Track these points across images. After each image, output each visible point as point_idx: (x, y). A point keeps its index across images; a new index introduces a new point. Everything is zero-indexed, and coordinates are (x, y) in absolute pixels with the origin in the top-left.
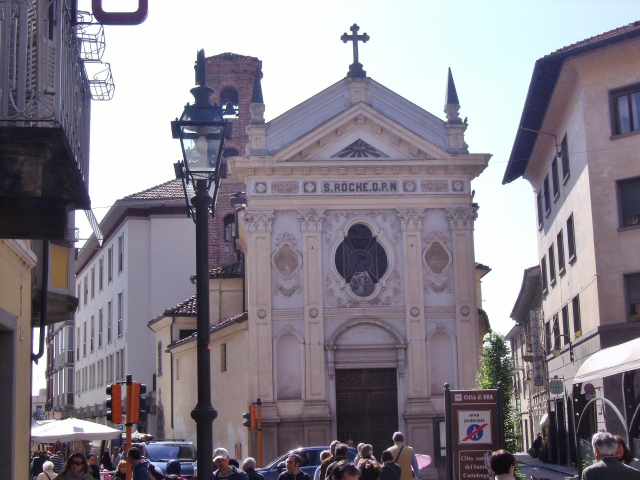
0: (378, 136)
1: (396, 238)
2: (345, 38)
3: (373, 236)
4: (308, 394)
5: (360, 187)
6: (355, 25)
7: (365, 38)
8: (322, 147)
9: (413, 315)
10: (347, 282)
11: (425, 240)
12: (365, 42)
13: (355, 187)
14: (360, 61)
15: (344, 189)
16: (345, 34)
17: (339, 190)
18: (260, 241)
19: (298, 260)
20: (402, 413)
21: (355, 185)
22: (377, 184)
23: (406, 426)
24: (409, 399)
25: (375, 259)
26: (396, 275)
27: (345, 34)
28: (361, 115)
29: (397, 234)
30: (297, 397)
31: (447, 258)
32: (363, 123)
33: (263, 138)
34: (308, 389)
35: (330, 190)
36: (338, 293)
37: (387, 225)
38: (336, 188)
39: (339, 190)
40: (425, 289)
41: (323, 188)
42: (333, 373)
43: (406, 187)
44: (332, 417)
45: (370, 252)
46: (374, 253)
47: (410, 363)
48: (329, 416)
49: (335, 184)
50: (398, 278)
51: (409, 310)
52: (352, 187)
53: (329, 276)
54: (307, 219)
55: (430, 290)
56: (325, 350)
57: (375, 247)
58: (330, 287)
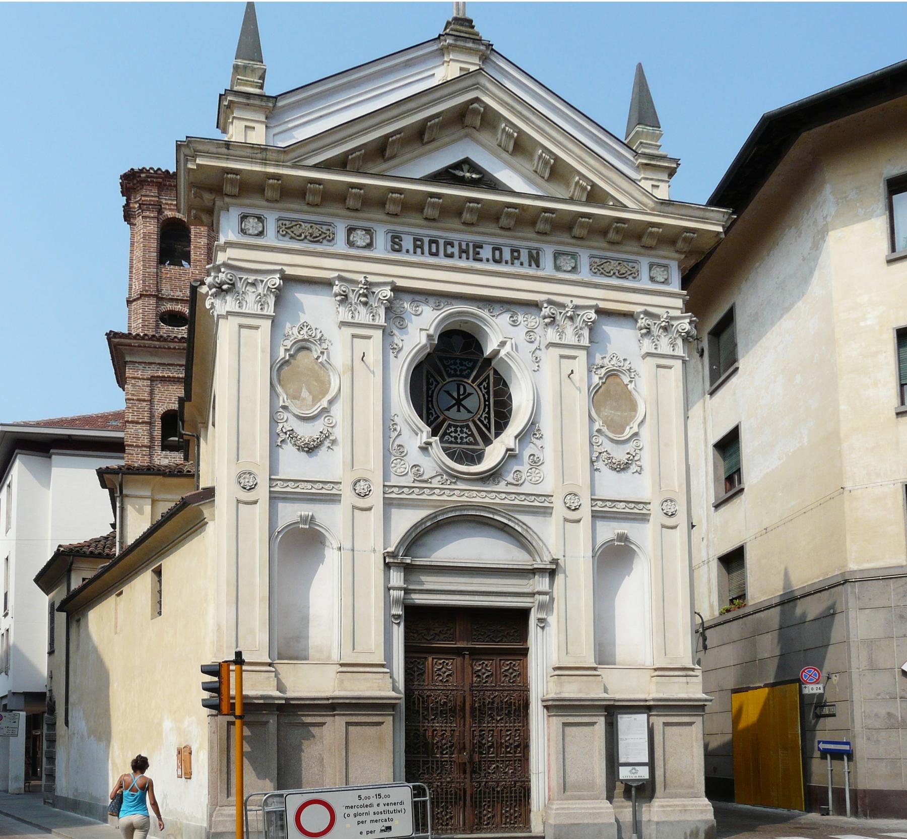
0: (505, 156)
3: (488, 352)
5: (466, 252)
10: (434, 434)
13: (456, 250)
17: (423, 253)
19: (330, 383)
21: (456, 244)
22: (500, 250)
25: (489, 400)
28: (477, 100)
35: (404, 250)
37: (519, 334)
38: (416, 247)
39: (423, 253)
41: (390, 243)
42: (399, 611)
43: (558, 262)
46: (488, 388)
49: (415, 240)
52: (450, 250)
56: (387, 566)
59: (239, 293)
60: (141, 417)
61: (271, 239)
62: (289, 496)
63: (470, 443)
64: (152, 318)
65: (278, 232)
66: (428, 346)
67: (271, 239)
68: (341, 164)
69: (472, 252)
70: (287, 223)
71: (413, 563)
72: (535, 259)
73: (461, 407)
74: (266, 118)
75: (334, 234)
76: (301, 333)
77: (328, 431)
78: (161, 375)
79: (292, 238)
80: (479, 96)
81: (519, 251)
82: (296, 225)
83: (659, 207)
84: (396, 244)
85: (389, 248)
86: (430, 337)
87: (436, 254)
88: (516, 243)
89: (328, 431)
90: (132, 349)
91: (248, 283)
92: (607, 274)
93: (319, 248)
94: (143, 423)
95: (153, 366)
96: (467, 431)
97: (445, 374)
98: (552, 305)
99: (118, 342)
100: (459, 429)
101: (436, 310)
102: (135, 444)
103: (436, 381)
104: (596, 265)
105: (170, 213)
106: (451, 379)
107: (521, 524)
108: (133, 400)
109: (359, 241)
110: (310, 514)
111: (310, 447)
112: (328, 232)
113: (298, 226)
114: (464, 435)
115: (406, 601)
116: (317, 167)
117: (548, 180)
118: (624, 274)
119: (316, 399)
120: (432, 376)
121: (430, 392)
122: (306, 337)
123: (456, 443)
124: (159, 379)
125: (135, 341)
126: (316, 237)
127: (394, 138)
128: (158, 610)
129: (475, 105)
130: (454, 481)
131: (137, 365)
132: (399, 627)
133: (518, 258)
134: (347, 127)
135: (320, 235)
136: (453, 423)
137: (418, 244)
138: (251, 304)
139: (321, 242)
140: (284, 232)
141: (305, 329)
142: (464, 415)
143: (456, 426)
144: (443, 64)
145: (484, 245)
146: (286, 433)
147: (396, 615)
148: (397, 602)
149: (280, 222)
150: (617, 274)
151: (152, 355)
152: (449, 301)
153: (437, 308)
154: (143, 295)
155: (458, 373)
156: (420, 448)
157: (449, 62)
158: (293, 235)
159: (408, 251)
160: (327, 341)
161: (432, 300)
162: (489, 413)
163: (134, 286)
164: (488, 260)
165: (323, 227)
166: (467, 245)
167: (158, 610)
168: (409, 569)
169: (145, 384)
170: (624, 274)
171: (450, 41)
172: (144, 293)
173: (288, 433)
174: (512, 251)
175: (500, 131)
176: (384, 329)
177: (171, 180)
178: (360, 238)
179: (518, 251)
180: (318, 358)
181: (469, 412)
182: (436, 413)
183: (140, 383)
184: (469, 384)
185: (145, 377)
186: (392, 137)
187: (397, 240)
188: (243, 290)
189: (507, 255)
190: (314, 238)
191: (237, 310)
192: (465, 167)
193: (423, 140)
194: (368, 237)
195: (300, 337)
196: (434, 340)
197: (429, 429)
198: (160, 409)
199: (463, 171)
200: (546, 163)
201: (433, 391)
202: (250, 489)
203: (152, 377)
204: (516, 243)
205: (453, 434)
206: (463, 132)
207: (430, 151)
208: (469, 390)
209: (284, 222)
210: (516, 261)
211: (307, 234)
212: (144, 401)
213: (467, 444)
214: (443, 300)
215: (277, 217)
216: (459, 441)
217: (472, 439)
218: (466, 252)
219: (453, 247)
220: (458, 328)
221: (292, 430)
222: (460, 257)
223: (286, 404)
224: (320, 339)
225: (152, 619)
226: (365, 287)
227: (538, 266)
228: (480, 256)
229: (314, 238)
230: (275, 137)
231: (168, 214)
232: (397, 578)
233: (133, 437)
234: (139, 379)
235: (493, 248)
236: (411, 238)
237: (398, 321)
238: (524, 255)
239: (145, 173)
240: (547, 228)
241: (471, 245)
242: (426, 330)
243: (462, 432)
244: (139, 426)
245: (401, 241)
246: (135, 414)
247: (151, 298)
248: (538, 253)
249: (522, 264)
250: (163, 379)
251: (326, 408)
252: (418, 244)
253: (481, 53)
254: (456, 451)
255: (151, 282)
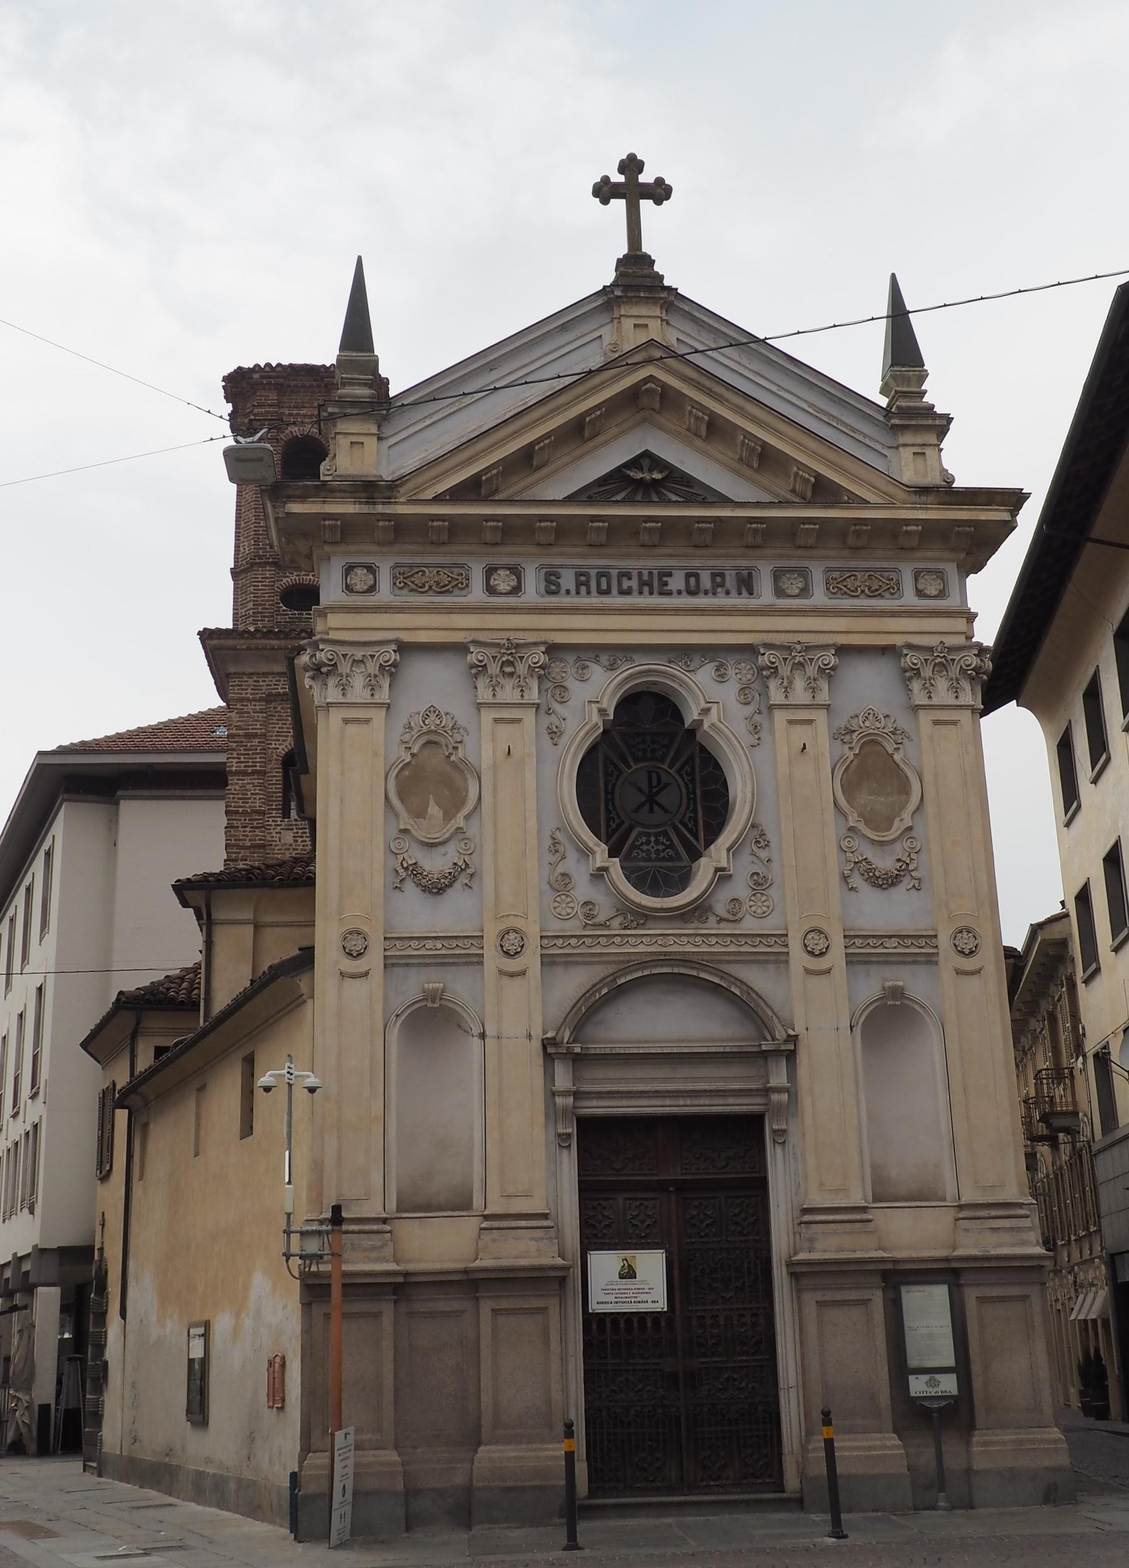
0: (698, 442)
1: (756, 729)
2: (604, 191)
3: (687, 723)
4: (493, 1195)
5: (650, 584)
6: (632, 158)
7: (660, 192)
8: (539, 468)
9: (811, 953)
10: (612, 854)
11: (842, 735)
12: (658, 202)
13: (634, 583)
14: (648, 247)
15: (604, 586)
16: (606, 180)
17: (589, 593)
18: (352, 729)
19: (467, 791)
20: (785, 1256)
21: (635, 574)
22: (697, 576)
23: (799, 1298)
24: (806, 1211)
25: (694, 792)
26: (757, 835)
27: (606, 180)
28: (651, 379)
29: (757, 717)
30: (460, 1204)
32: (657, 405)
34: (493, 1180)
35: (563, 591)
36: (583, 889)
37: (728, 693)
38: (579, 584)
39: (589, 593)
40: (845, 878)
41: (543, 585)
42: (572, 1129)
45: (679, 771)
46: (692, 774)
47: (806, 1101)
48: (559, 1261)
49: (578, 575)
50: (762, 844)
51: (801, 934)
52: (626, 584)
53: (559, 835)
54: (494, 669)
55: (857, 880)
57: (691, 758)
58: (560, 869)
60: (250, 764)
63: (671, 859)
64: (268, 601)
66: (601, 724)
68: (471, 490)
69: (656, 583)
72: (746, 584)
73: (654, 805)
75: (468, 580)
76: (427, 722)
78: (281, 691)
83: (914, 498)
84: (552, 585)
85: (542, 590)
86: (602, 712)
87: (607, 592)
89: (464, 861)
92: (851, 594)
94: (253, 773)
98: (772, 649)
100: (652, 839)
104: (835, 582)
106: (639, 766)
107: (738, 984)
109: (502, 584)
111: (440, 886)
112: (460, 578)
114: (661, 847)
117: (756, 471)
118: (877, 590)
119: (448, 816)
120: (612, 763)
121: (610, 787)
122: (433, 728)
123: (650, 860)
125: (242, 642)
126: (445, 586)
128: (247, 1128)
129: (649, 385)
130: (641, 922)
133: (722, 585)
139: (451, 592)
141: (433, 717)
143: (648, 835)
144: (612, 321)
145: (673, 571)
146: (406, 869)
147: (563, 1134)
150: (867, 591)
153: (612, 667)
155: (649, 755)
157: (619, 318)
159: (568, 592)
162: (695, 811)
163: (241, 549)
164: (679, 592)
165: (453, 569)
166: (650, 574)
167: (247, 1128)
168: (579, 1061)
169: (258, 708)
170: (877, 590)
171: (618, 293)
174: (714, 576)
175: (687, 414)
178: (503, 580)
179: (722, 575)
180: (448, 757)
181: (666, 811)
187: (553, 578)
189: (706, 581)
192: (646, 463)
193: (583, 437)
198: (281, 747)
199: (641, 470)
200: (753, 450)
202: (358, 955)
205: (645, 847)
206: (639, 416)
207: (596, 448)
210: (719, 590)
212: (255, 736)
213: (664, 859)
219: (630, 579)
221: (416, 863)
222: (641, 593)
224: (453, 728)
225: (241, 1139)
227: (751, 593)
228: (669, 588)
231: (293, 430)
232: (563, 1078)
234: (248, 700)
238: (730, 581)
239: (257, 372)
244: (247, 780)
245: (559, 578)
246: (242, 760)
248: (750, 575)
249: (728, 593)
251: (462, 828)
252: (582, 583)
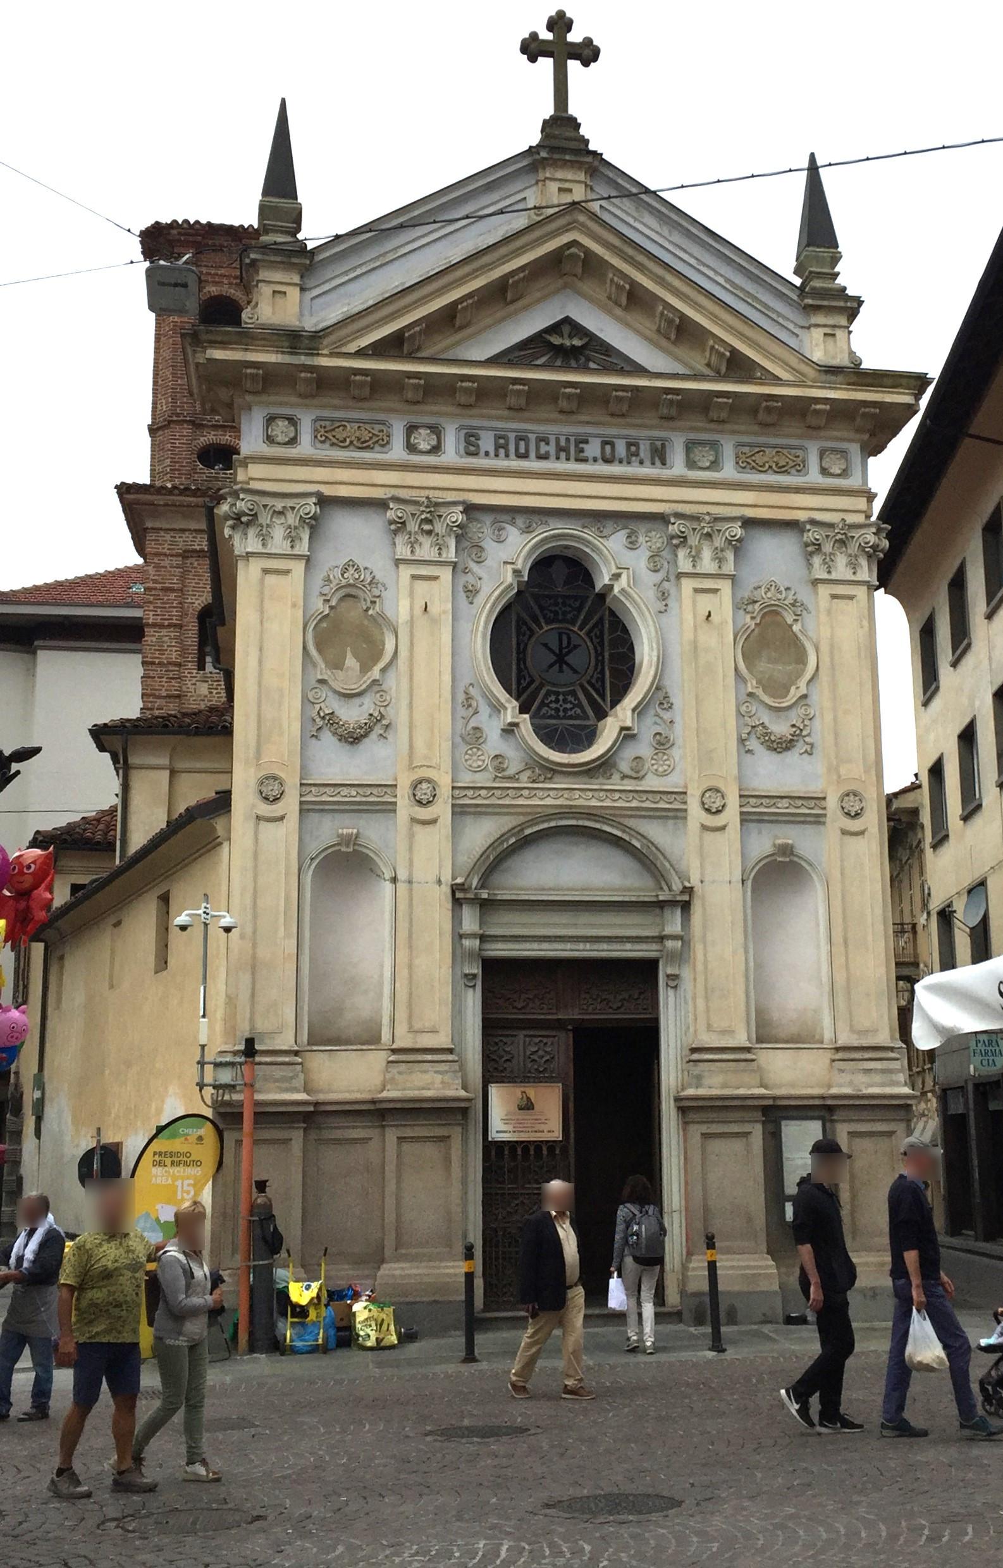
0: (618, 312)
1: (664, 596)
2: (532, 48)
3: (598, 587)
4: (401, 1029)
5: (565, 450)
6: (561, 14)
7: (588, 53)
8: (461, 328)
9: (708, 810)
10: (523, 710)
12: (586, 64)
13: (552, 449)
14: (574, 109)
15: (522, 450)
16: (534, 36)
17: (507, 456)
22: (612, 444)
23: (684, 1130)
24: (694, 1050)
26: (659, 697)
27: (534, 36)
28: (574, 243)
29: (666, 584)
31: (802, 659)
32: (579, 271)
33: (294, 293)
34: (401, 1015)
35: (482, 453)
36: (494, 742)
37: (639, 560)
38: (497, 447)
39: (507, 456)
40: (742, 741)
41: (463, 445)
42: (476, 969)
43: (692, 456)
44: (469, 1100)
45: (588, 634)
46: (601, 636)
47: (698, 949)
50: (665, 706)
51: (698, 793)
52: (544, 448)
53: (473, 691)
54: (413, 526)
55: (753, 744)
56: (457, 903)
57: (601, 619)
58: (472, 724)
59: (262, 527)
60: (166, 617)
61: (306, 446)
62: (327, 807)
63: (577, 717)
64: (185, 458)
65: (316, 437)
66: (515, 586)
67: (306, 446)
68: (393, 346)
69: (573, 449)
70: (328, 423)
71: (492, 898)
72: (660, 455)
73: (564, 666)
74: (302, 277)
75: (389, 436)
76: (346, 575)
77: (380, 712)
78: (198, 548)
79: (333, 444)
80: (578, 239)
81: (638, 443)
82: (339, 427)
84: (471, 447)
85: (462, 451)
86: (517, 573)
87: (525, 456)
88: (633, 432)
89: (380, 712)
90: (155, 511)
91: (275, 511)
92: (759, 469)
93: (367, 456)
94: (169, 626)
95: (187, 534)
96: (573, 700)
97: (542, 621)
98: (681, 519)
99: (135, 499)
100: (561, 697)
101: (528, 532)
102: (157, 661)
103: (530, 629)
104: (744, 456)
105: (214, 289)
106: (549, 627)
107: (639, 837)
108: (155, 589)
109: (422, 442)
110: (355, 831)
111: (355, 736)
112: (381, 434)
113: (341, 428)
114: (569, 706)
115: (483, 952)
116: (361, 353)
117: (674, 343)
118: (784, 466)
119: (365, 668)
120: (525, 623)
121: (522, 647)
122: (351, 581)
123: (557, 717)
124: (195, 555)
125: (159, 497)
126: (366, 441)
127: (465, 304)
129: (573, 250)
130: (549, 776)
131: (162, 533)
132: (474, 990)
133: (637, 454)
134: (403, 297)
135: (371, 438)
136: (554, 689)
137: (501, 446)
138: (278, 542)
139: (372, 448)
140: (324, 438)
141: (351, 570)
142: (567, 676)
143: (557, 694)
144: (537, 183)
145: (590, 439)
146: (323, 718)
147: (469, 975)
148: (471, 954)
149: (318, 424)
150: (774, 467)
151: (185, 516)
152: (544, 519)
153: (527, 530)
154: (172, 421)
155: (560, 617)
156: (503, 730)
157: (544, 181)
158: (334, 440)
159: (487, 454)
160: (379, 585)
161: (520, 521)
162: (602, 672)
163: (159, 406)
164: (595, 460)
165: (374, 426)
166: (568, 440)
168: (487, 906)
169: (174, 563)
170: (784, 466)
171: (544, 154)
172: (175, 418)
173: (327, 718)
174: (629, 445)
175: (608, 281)
176: (455, 565)
177: (216, 237)
178: (424, 440)
179: (637, 445)
180: (367, 610)
181: (575, 671)
182: (530, 676)
183: (166, 562)
184: (574, 632)
185: (174, 552)
186: (461, 303)
187: (472, 439)
188: (268, 522)
189: (621, 449)
190: (363, 443)
191: (260, 549)
192: (566, 329)
193: (506, 299)
194: (435, 437)
195: (344, 582)
196: (522, 576)
197: (516, 704)
198: (197, 602)
199: (562, 336)
200: (670, 322)
201: (526, 645)
203: (185, 551)
204: (633, 432)
205: (553, 705)
206: (560, 282)
207: (516, 312)
208: (575, 640)
209: (323, 423)
210: (634, 458)
211: (353, 438)
212: (172, 590)
213: (571, 718)
214: (536, 518)
215: (314, 417)
216: (561, 714)
217: (579, 711)
218: (565, 450)
219: (548, 444)
220: (558, 553)
221: (333, 713)
222: (558, 458)
223: (325, 677)
224: (370, 583)
226: (428, 510)
227: (664, 464)
228: (585, 454)
229: (363, 443)
230: (314, 301)
231: (211, 290)
232: (470, 921)
233: (155, 650)
234: (165, 555)
235: (602, 442)
236: (491, 434)
237: (475, 550)
238: (644, 450)
240: (674, 412)
241: (572, 439)
242: (513, 563)
243: (565, 701)
244: (164, 632)
245: (478, 439)
246: (159, 613)
247: (185, 426)
248: (663, 445)
249: (641, 462)
250: (201, 554)
251: (378, 681)
252: (501, 446)
253: (587, 166)
254: (556, 730)
255: (185, 400)
